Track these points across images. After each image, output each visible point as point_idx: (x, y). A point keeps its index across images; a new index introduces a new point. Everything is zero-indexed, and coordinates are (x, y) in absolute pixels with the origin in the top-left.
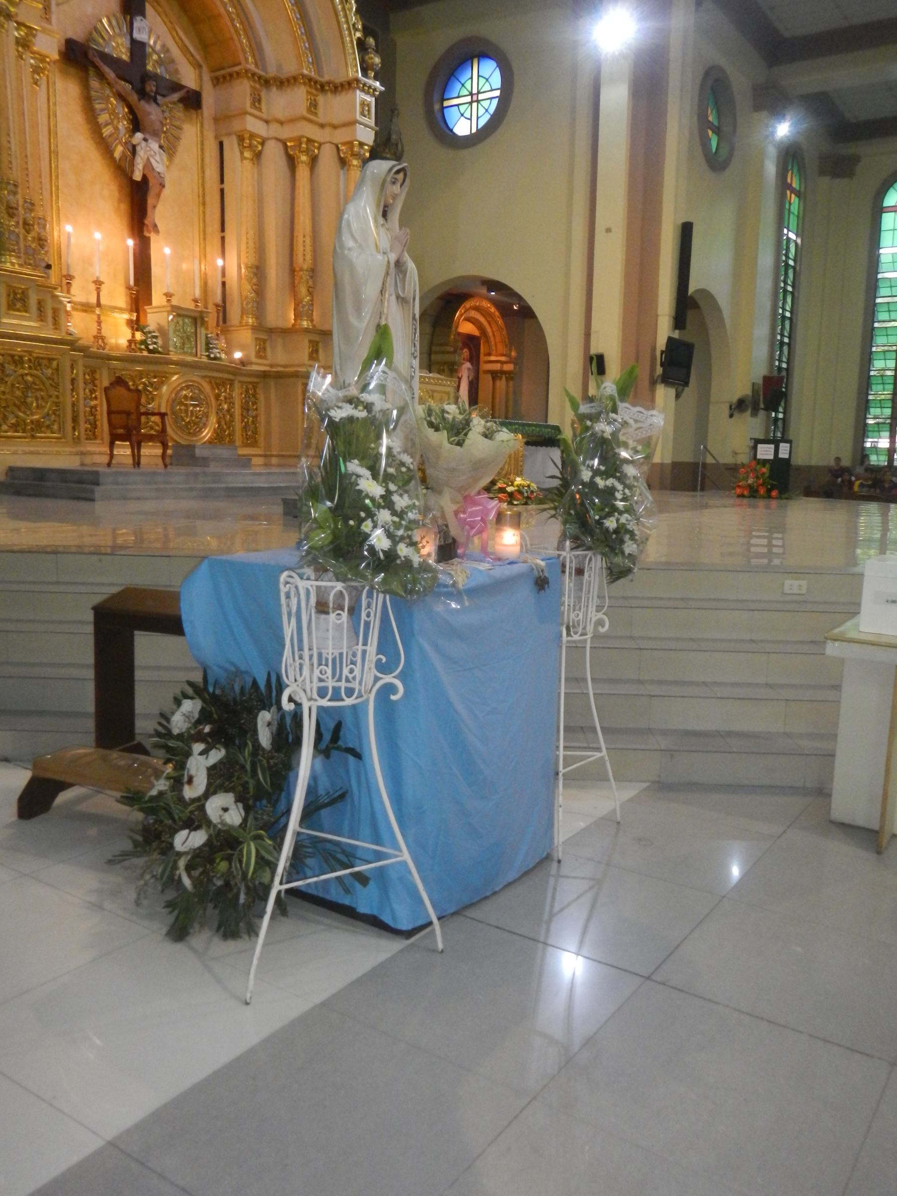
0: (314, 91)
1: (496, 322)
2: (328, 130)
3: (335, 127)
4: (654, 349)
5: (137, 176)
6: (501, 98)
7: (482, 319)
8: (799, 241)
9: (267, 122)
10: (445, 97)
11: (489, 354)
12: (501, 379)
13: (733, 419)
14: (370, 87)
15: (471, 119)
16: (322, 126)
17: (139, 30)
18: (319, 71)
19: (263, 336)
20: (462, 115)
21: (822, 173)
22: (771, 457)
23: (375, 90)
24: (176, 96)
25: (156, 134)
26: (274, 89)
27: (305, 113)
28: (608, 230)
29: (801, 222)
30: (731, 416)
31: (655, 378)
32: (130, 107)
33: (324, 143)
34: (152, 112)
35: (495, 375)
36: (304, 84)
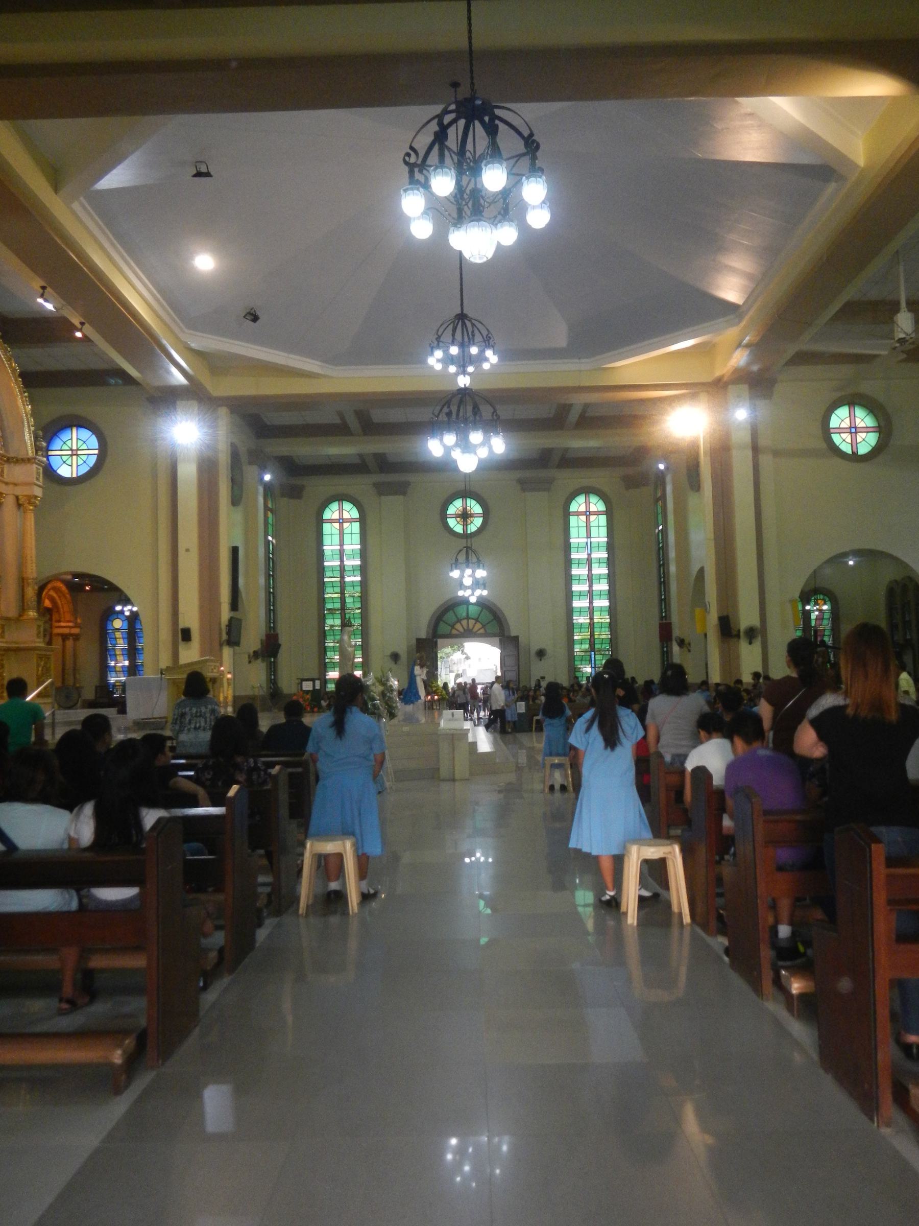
1: (64, 595)
2: (11, 486)
3: (15, 485)
4: (220, 624)
6: (98, 455)
7: (55, 595)
8: (274, 541)
10: (50, 448)
11: (59, 621)
12: (68, 639)
13: (251, 664)
15: (71, 466)
16: (7, 484)
20: (64, 462)
21: (283, 495)
22: (311, 689)
28: (187, 550)
29: (274, 529)
30: (250, 662)
31: (222, 642)
35: (65, 637)
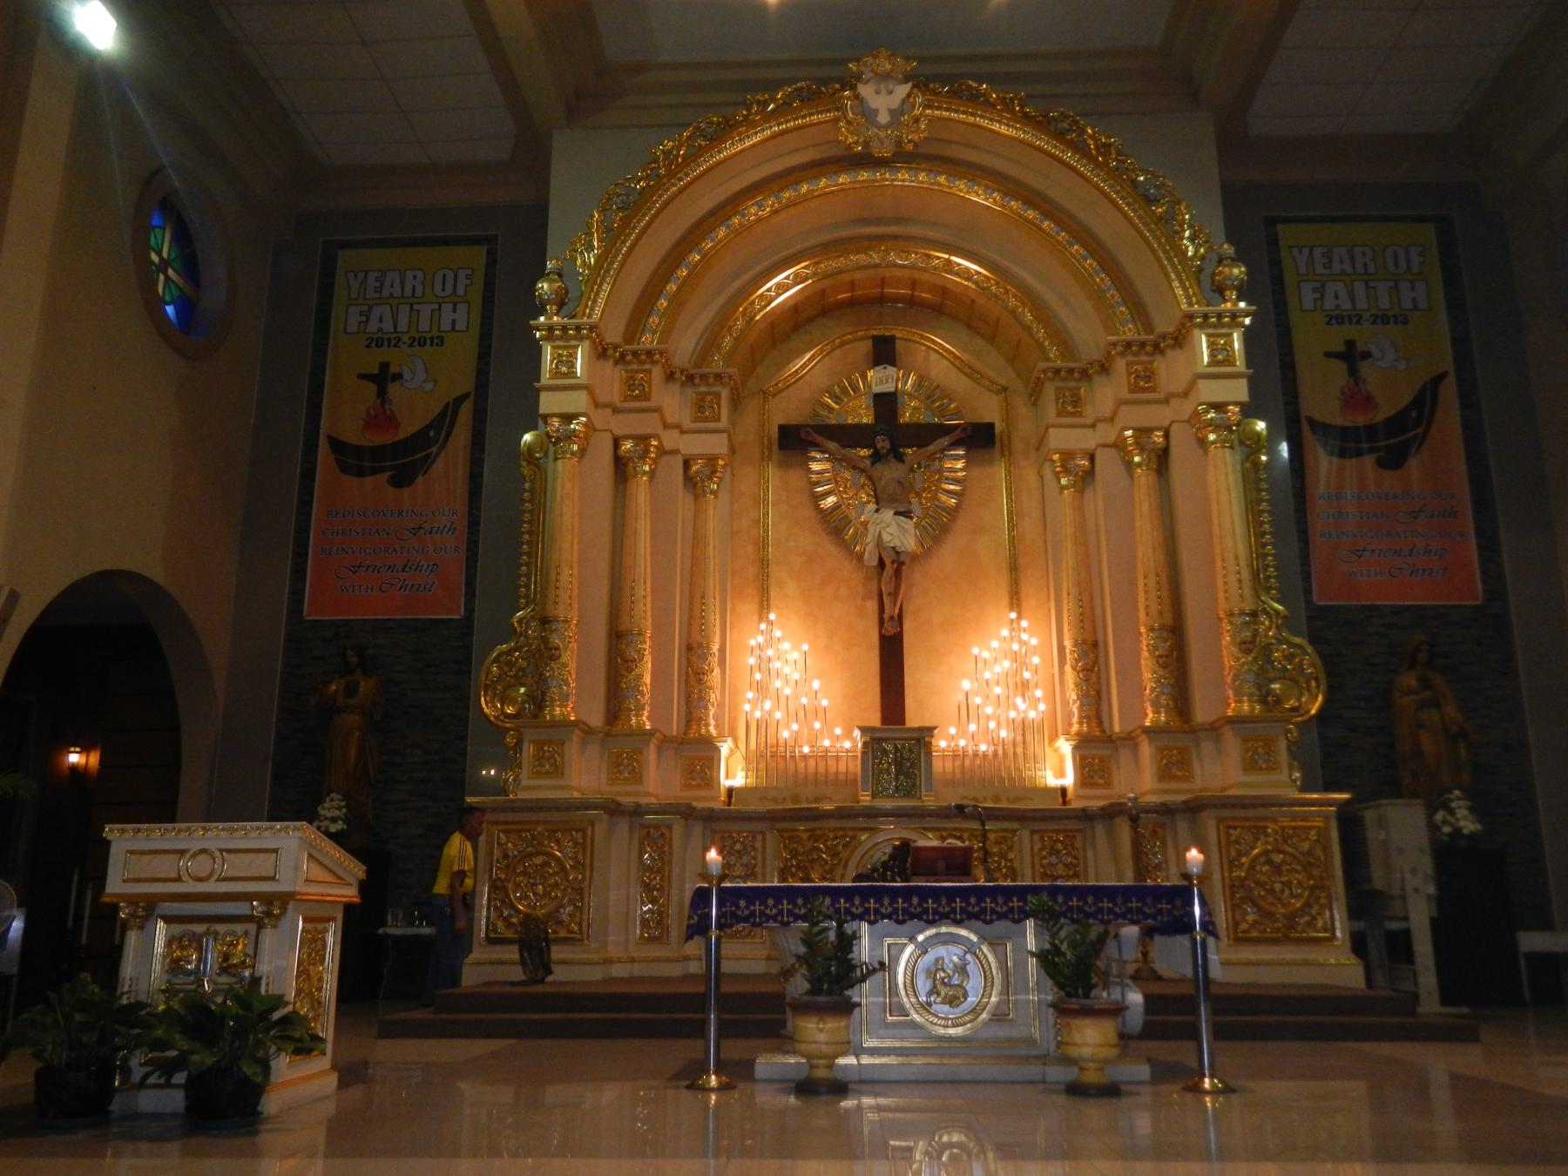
0: (1144, 358)
5: (871, 559)
9: (1093, 426)
14: (1220, 316)
17: (881, 381)
18: (1148, 327)
19: (1105, 751)
23: (1234, 315)
24: (945, 441)
25: (892, 500)
26: (1097, 380)
27: (1125, 395)
32: (870, 478)
33: (1170, 425)
34: (890, 472)
36: (1122, 354)
